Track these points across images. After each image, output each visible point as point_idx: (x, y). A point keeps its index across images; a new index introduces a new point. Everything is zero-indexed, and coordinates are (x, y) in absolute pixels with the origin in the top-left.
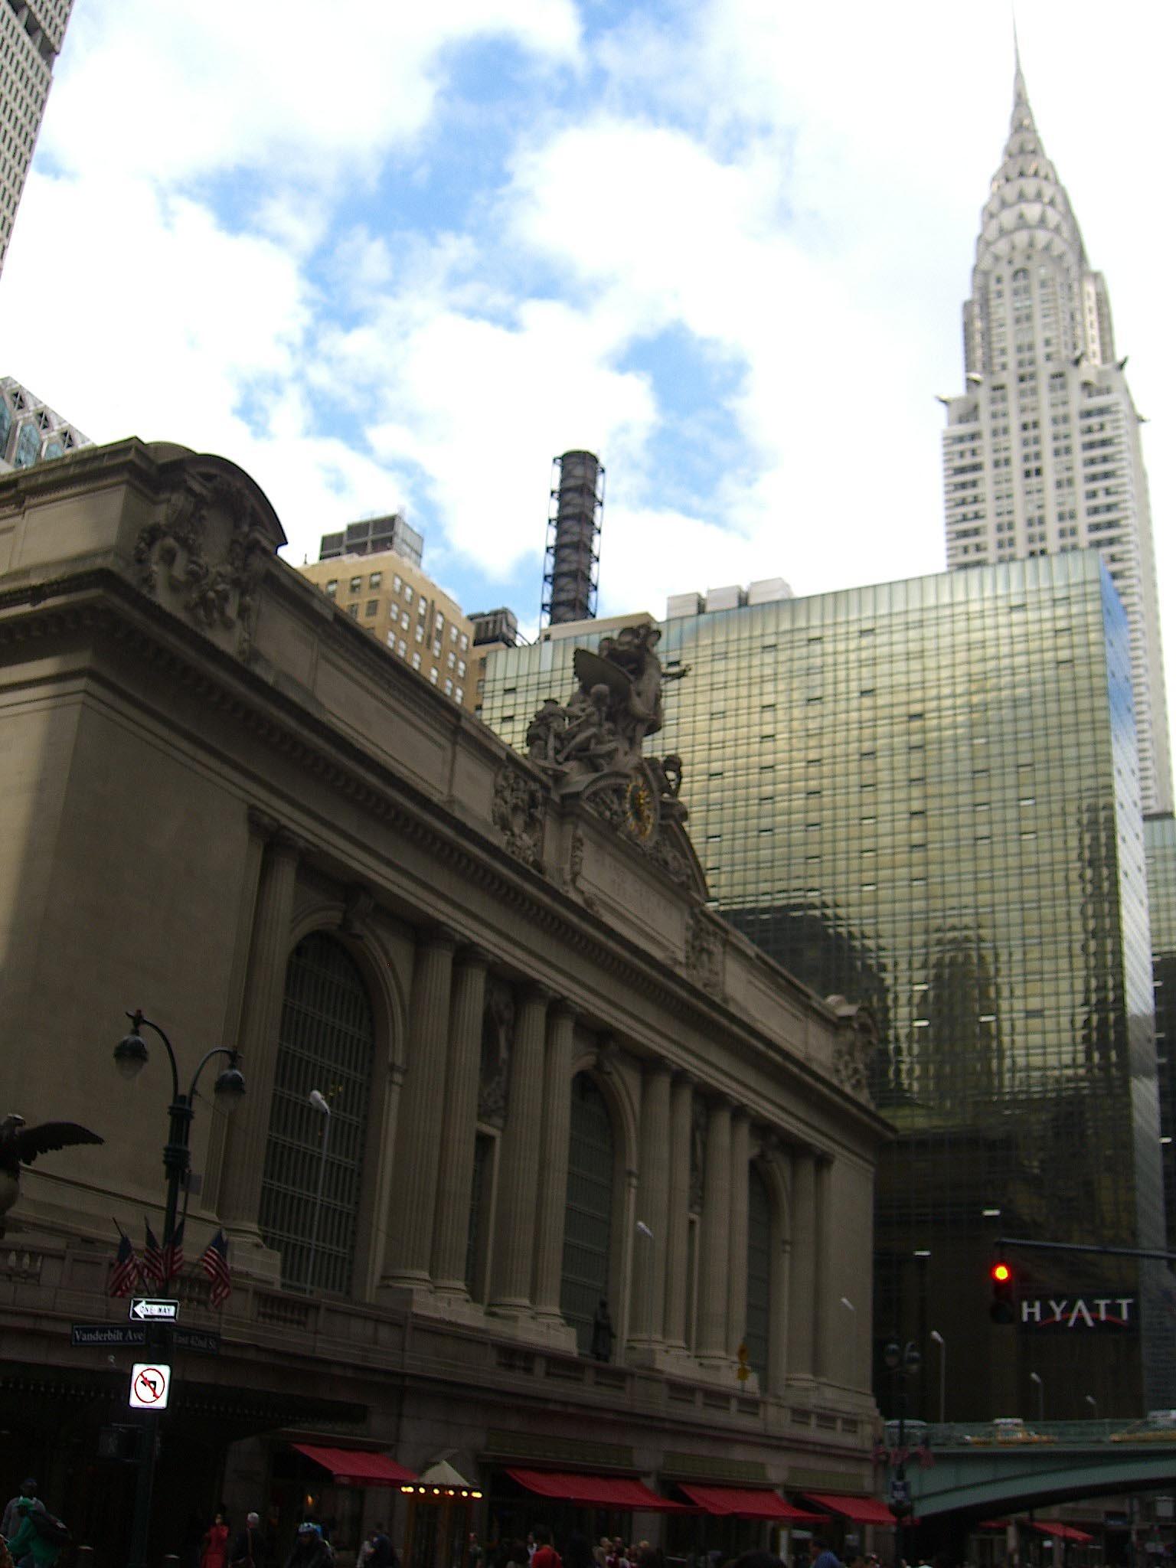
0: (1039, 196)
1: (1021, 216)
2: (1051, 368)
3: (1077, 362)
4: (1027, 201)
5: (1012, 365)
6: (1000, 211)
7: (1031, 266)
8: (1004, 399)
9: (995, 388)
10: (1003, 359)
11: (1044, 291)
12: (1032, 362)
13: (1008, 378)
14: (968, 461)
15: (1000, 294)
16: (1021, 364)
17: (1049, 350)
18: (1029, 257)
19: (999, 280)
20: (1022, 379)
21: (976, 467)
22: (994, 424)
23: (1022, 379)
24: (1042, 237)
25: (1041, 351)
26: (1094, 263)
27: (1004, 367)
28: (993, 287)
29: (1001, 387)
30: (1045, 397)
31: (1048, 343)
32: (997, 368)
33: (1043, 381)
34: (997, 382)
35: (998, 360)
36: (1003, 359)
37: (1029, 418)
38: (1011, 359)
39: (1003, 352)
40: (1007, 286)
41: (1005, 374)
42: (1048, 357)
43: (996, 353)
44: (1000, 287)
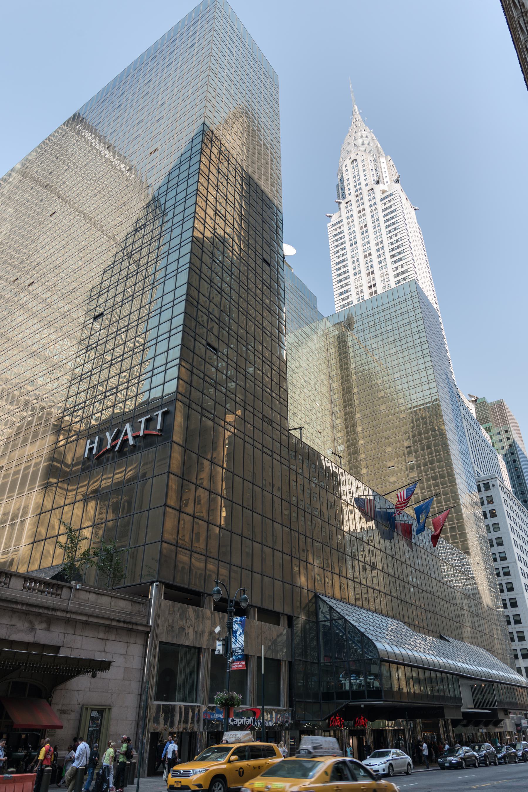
0: (362, 137)
2: (368, 188)
7: (358, 158)
12: (360, 189)
13: (352, 198)
15: (347, 171)
19: (346, 166)
22: (347, 215)
23: (357, 196)
24: (362, 148)
27: (350, 194)
28: (344, 169)
34: (347, 200)
35: (347, 193)
40: (350, 167)
42: (367, 185)
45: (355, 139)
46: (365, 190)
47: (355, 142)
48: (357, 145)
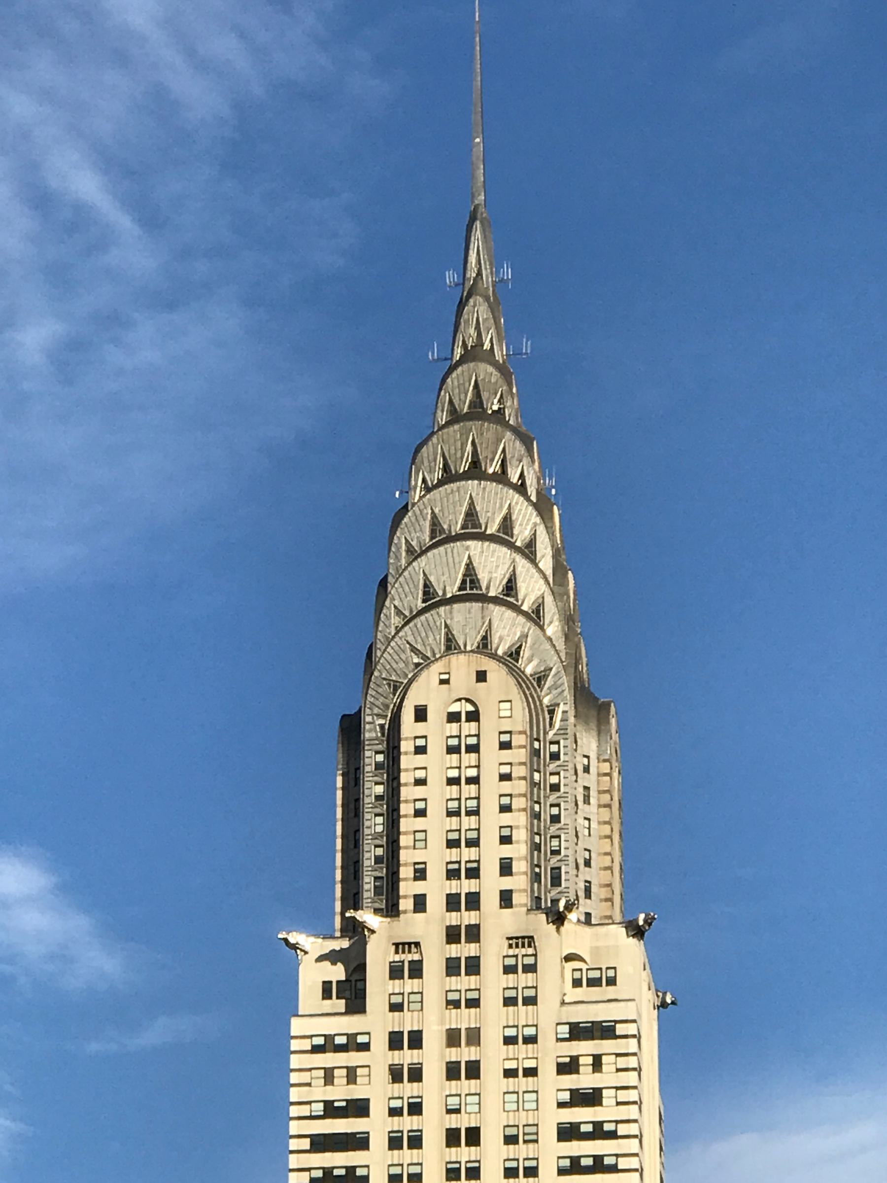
3: (558, 919)
4: (482, 537)
5: (436, 903)
8: (416, 970)
9: (399, 947)
10: (419, 887)
11: (506, 755)
12: (474, 901)
13: (427, 928)
14: (340, 1093)
16: (453, 902)
17: (507, 883)
18: (481, 676)
19: (421, 714)
20: (453, 935)
21: (359, 1108)
23: (453, 935)
25: (490, 884)
27: (420, 903)
28: (408, 726)
30: (493, 983)
31: (506, 868)
32: (406, 904)
33: (493, 951)
35: (408, 888)
36: (419, 887)
37: (464, 1019)
38: (436, 888)
39: (420, 874)
41: (420, 916)
42: (506, 899)
43: (406, 872)
44: (421, 728)
46: (497, 925)
48: (483, 576)
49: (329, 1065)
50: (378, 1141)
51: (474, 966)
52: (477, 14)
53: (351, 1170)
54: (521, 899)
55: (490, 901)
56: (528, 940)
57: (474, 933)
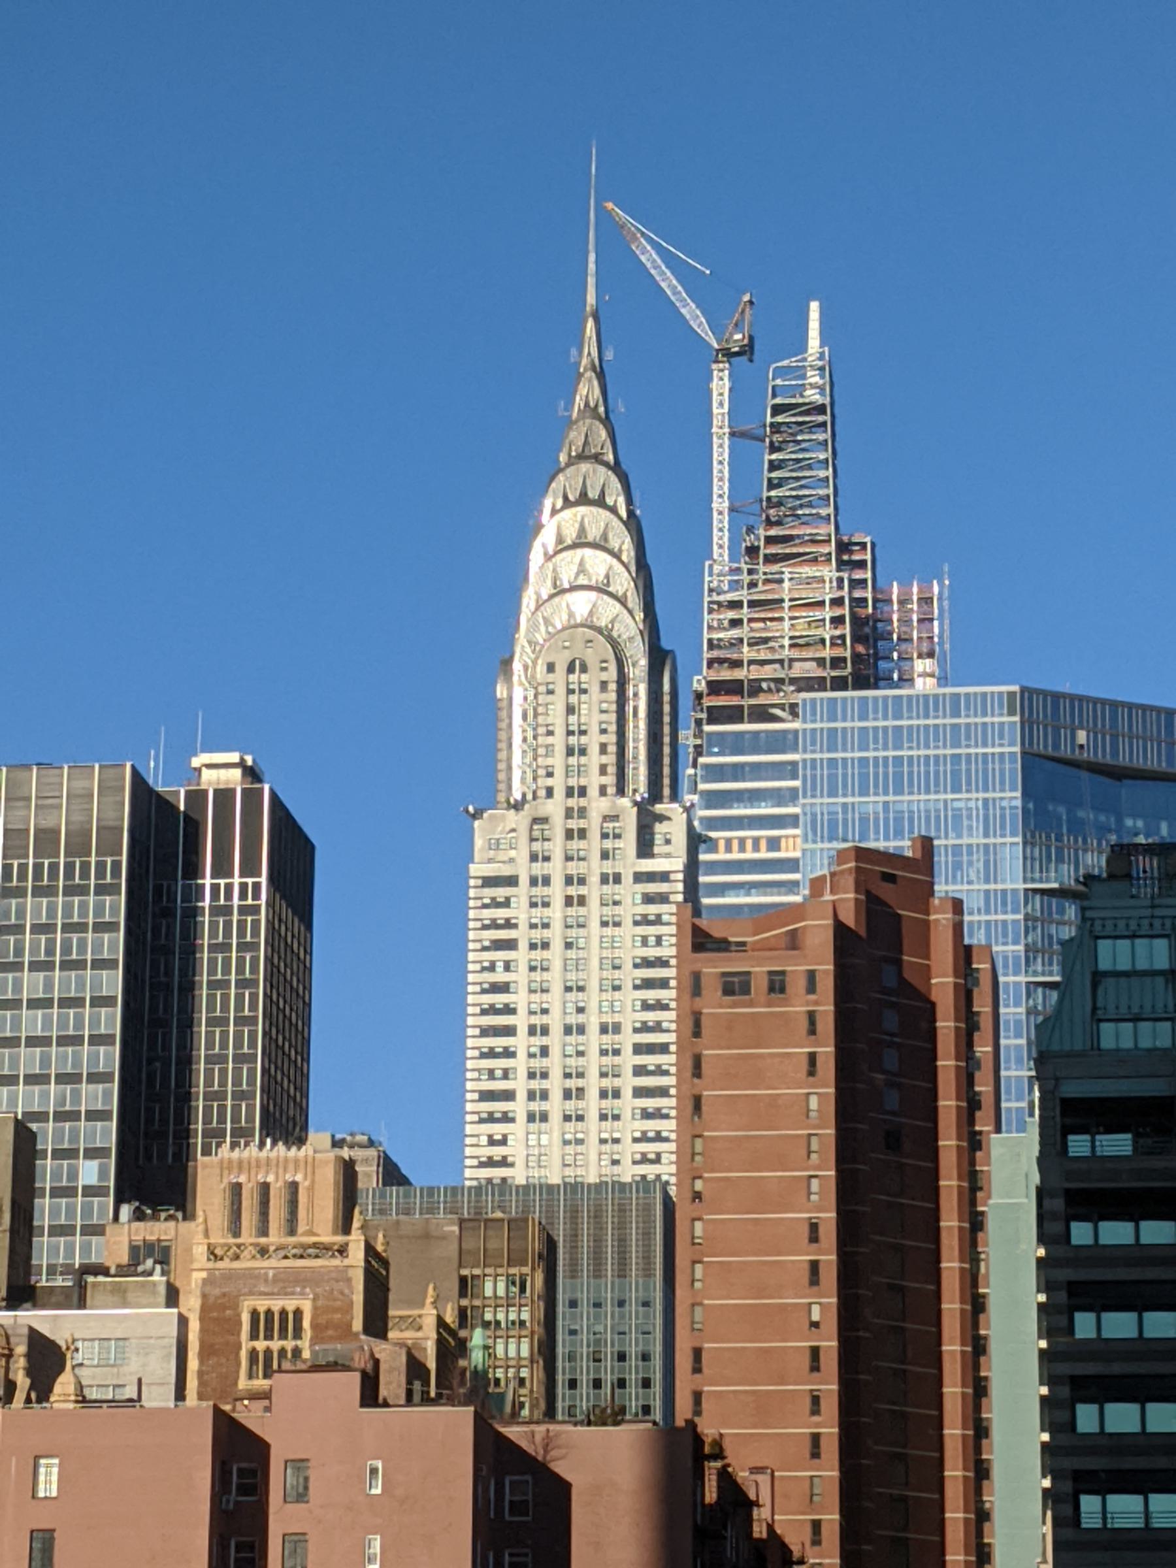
1: (582, 570)
5: (559, 793)
6: (556, 553)
9: (535, 821)
10: (550, 782)
20: (569, 813)
26: (665, 644)
29: (545, 820)
33: (594, 823)
36: (550, 782)
41: (549, 801)
42: (603, 791)
45: (582, 531)
47: (588, 552)
49: (491, 1067)
50: (522, 1030)
51: (582, 834)
52: (592, 257)
53: (504, 1180)
54: (611, 790)
55: (593, 792)
56: (615, 818)
57: (583, 812)
